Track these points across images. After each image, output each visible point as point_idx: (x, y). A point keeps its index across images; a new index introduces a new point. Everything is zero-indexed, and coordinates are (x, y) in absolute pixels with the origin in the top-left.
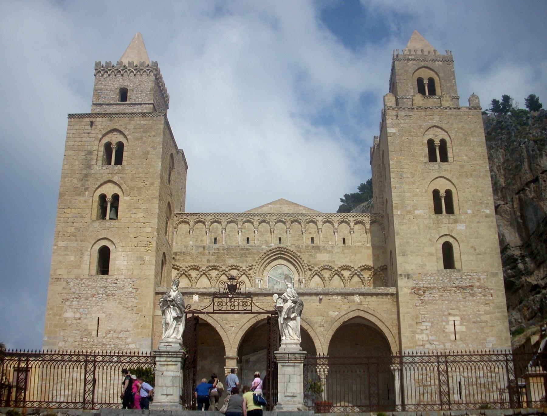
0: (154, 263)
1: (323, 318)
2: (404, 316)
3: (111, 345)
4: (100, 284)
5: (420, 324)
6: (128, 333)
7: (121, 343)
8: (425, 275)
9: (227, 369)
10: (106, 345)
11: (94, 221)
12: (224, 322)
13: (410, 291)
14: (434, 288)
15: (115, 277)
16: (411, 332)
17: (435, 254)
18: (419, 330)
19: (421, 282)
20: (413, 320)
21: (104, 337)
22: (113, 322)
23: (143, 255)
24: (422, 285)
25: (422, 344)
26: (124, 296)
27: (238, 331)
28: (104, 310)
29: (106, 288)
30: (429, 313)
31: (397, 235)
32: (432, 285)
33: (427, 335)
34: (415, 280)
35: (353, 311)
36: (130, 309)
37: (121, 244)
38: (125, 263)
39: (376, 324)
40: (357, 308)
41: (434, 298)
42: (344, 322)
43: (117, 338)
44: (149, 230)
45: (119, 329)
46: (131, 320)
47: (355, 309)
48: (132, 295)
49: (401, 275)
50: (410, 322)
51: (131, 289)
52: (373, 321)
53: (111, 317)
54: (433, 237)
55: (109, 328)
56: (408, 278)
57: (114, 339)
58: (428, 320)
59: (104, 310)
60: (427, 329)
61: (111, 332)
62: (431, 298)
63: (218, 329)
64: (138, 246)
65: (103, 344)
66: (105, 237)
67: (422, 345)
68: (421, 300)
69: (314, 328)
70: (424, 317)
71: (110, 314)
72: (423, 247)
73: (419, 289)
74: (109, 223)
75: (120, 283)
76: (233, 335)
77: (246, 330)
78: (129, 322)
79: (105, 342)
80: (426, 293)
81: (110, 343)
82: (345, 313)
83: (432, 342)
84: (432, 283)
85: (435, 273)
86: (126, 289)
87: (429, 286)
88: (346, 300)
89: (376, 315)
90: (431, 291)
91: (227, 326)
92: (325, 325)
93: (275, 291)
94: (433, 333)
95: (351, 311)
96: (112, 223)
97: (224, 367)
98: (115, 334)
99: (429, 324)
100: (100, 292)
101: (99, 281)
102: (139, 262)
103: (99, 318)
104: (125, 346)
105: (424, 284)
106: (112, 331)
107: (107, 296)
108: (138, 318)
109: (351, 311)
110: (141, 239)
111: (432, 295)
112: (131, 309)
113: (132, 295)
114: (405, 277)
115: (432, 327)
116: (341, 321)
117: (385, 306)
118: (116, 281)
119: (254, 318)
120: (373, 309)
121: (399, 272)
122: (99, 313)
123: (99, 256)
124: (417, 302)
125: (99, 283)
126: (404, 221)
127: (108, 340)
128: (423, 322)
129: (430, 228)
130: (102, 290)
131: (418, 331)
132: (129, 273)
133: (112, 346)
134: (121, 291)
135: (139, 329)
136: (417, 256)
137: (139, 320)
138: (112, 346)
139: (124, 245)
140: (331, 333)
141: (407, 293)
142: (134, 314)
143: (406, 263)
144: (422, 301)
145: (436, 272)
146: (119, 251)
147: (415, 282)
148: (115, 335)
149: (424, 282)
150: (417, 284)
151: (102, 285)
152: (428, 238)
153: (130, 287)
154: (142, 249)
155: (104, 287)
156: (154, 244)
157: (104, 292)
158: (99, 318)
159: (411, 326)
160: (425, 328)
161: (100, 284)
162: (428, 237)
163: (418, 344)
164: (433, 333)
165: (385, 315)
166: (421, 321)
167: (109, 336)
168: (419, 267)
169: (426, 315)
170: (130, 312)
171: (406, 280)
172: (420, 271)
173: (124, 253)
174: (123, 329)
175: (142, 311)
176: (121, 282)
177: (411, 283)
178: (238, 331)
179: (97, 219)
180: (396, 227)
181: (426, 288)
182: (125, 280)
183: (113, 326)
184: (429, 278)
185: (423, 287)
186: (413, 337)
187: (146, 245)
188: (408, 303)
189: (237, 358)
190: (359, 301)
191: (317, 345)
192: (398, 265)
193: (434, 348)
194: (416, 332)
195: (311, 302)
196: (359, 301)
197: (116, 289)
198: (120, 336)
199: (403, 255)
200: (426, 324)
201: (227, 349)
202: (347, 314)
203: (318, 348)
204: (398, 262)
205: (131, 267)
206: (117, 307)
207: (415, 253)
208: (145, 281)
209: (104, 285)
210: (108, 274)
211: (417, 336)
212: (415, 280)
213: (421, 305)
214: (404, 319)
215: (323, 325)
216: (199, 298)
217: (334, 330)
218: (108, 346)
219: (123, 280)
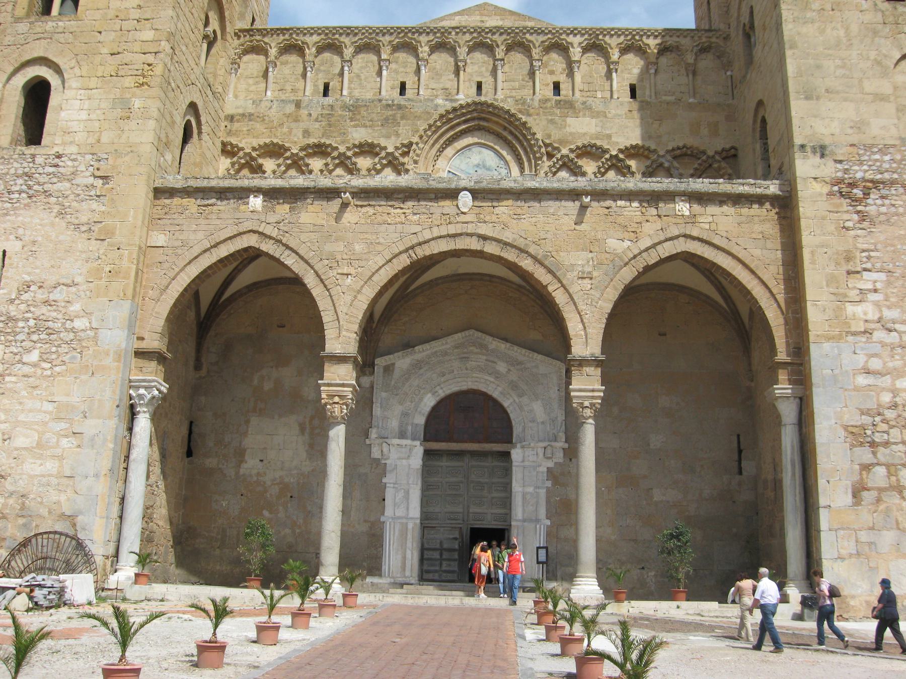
0: (155, 114)
1: (590, 255)
2: (812, 253)
3: (27, 320)
4: (16, 169)
5: (858, 276)
6: (73, 289)
7: (54, 314)
8: (868, 148)
9: (326, 388)
10: (17, 320)
11: (18, 20)
12: (326, 262)
13: (826, 189)
14: (893, 182)
15: (56, 149)
16: (833, 298)
17: (892, 98)
18: (858, 292)
19: (856, 168)
20: (837, 264)
21: (12, 301)
22: (38, 263)
23: (128, 96)
24: (859, 175)
25: (862, 330)
26: (72, 197)
27: (362, 287)
28: (21, 231)
29: (29, 176)
30: (879, 247)
31: (791, 48)
32: (887, 176)
33: (877, 304)
34: (840, 162)
35: (671, 239)
36: (83, 228)
37: (77, 71)
38: (84, 116)
39: (734, 273)
40: (682, 231)
41: (893, 209)
42: (648, 269)
43: (46, 302)
44: (148, 35)
45: (52, 280)
46: (84, 256)
47: (677, 233)
48: (93, 193)
49: (803, 146)
50: (827, 270)
51: (91, 180)
52: (724, 266)
53: (34, 249)
54: (885, 56)
55: (27, 278)
56: (823, 156)
57: (35, 306)
58: (878, 265)
59: (21, 231)
60: (876, 291)
61: (33, 288)
62: (883, 209)
63: (310, 280)
64: (120, 75)
65: (10, 319)
66: (41, 54)
67: (865, 332)
68: (858, 212)
69: (564, 282)
70: (869, 258)
71: (34, 242)
72: (860, 81)
73: (852, 185)
74: (54, 24)
75: (67, 166)
76: (348, 298)
77: (382, 284)
78: (80, 262)
79: (13, 314)
80: (872, 196)
81: (27, 315)
82: (648, 243)
83: (889, 325)
84: (887, 171)
85: (894, 146)
86: (79, 180)
87: (879, 176)
88: (653, 211)
89: (733, 251)
90: (884, 192)
91: (332, 273)
92: (595, 274)
93: (463, 184)
94: (892, 300)
95: (667, 240)
96: (60, 24)
97: (319, 382)
98: (40, 291)
99: (882, 276)
100: (14, 188)
101: (15, 160)
102: (118, 112)
103: (4, 252)
104: (64, 324)
105: (866, 171)
106: (35, 284)
107: (30, 197)
108: (101, 252)
109: (667, 240)
110: (127, 57)
111: (887, 202)
112: (87, 229)
113: (93, 193)
114: (814, 152)
115: (889, 283)
116: (640, 264)
117: (758, 228)
118: (57, 160)
119: (404, 256)
120: (724, 234)
121: (798, 140)
122: (7, 240)
123: (26, 103)
124: (846, 216)
125: (16, 165)
126: (809, 15)
127: (23, 307)
128: (865, 270)
129: (875, 33)
130: (20, 181)
131: (853, 294)
132: (91, 140)
133: (32, 323)
134: (67, 185)
135: (101, 278)
136: (846, 100)
137: (104, 257)
138: (32, 323)
139: (84, 74)
140: (612, 294)
141: (821, 194)
142: (93, 242)
143: (815, 116)
144: (863, 217)
145: (897, 142)
146: (70, 88)
147: (839, 166)
148: (41, 295)
149: (865, 167)
150: (846, 171)
151: (20, 172)
152: (872, 58)
153: (88, 174)
154: (129, 82)
155: (26, 174)
156: (159, 70)
157: (24, 187)
158: (4, 252)
159: (831, 280)
160: (870, 286)
161: (16, 169)
162: (873, 55)
163: (853, 329)
164: (892, 300)
165: (757, 252)
166: (859, 269)
167: (25, 297)
168: (851, 127)
169: (872, 254)
170: (85, 235)
171: (817, 159)
172: (854, 139)
173: (83, 91)
174: (61, 281)
175: (113, 234)
176: (70, 163)
177: (829, 169)
178: (362, 287)
179: (28, 15)
180: (788, 29)
181: (872, 181)
182: (79, 158)
183: (37, 271)
184: (877, 157)
185: (864, 180)
186: (839, 311)
187: (139, 72)
188: (823, 218)
189: (355, 358)
190: (687, 213)
191: (573, 326)
192: (795, 122)
193: (897, 340)
194: (846, 296)
195: (561, 213)
196: (687, 213)
197: (55, 180)
198: (52, 297)
199: (807, 98)
200: (874, 276)
201: (330, 333)
202: (654, 246)
203: (576, 336)
204: (793, 113)
205: (97, 124)
206: (52, 225)
207: (838, 92)
208: (127, 159)
209: (27, 170)
210: (39, 143)
211: (850, 309)
212: (840, 162)
213: (858, 225)
214: (813, 262)
215: (590, 273)
216: (265, 201)
217: (621, 287)
218: (21, 324)
219: (73, 157)
